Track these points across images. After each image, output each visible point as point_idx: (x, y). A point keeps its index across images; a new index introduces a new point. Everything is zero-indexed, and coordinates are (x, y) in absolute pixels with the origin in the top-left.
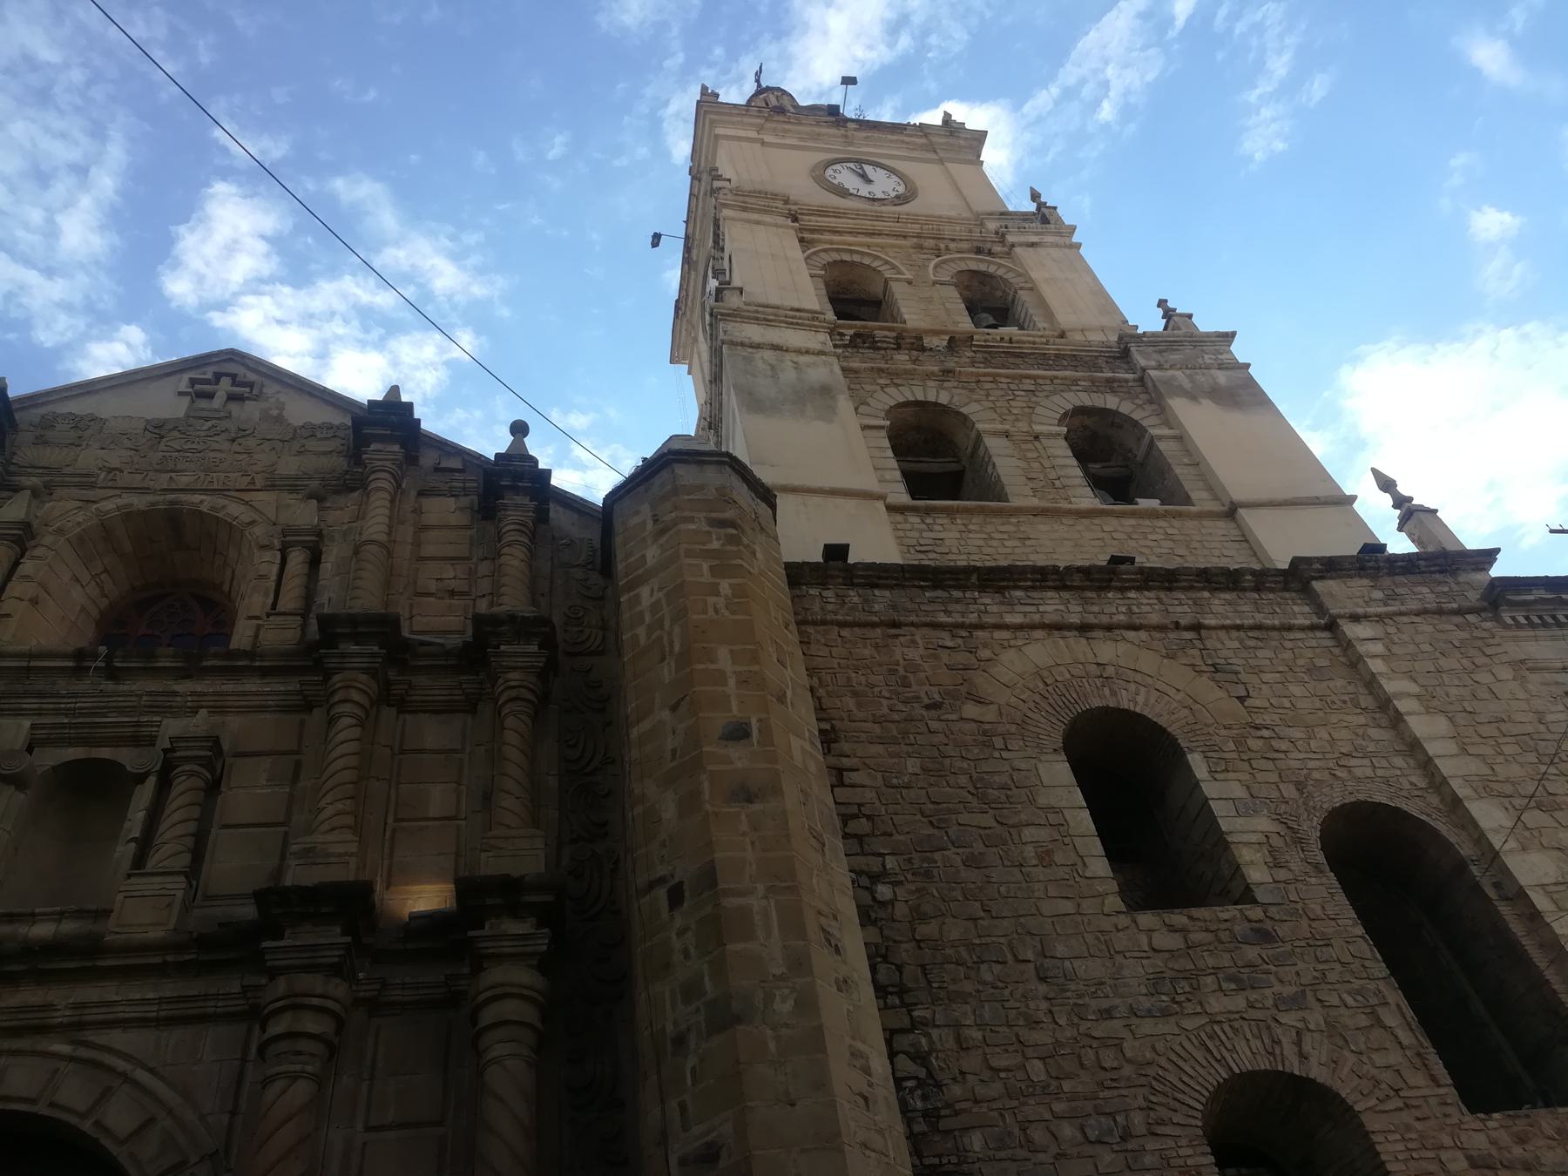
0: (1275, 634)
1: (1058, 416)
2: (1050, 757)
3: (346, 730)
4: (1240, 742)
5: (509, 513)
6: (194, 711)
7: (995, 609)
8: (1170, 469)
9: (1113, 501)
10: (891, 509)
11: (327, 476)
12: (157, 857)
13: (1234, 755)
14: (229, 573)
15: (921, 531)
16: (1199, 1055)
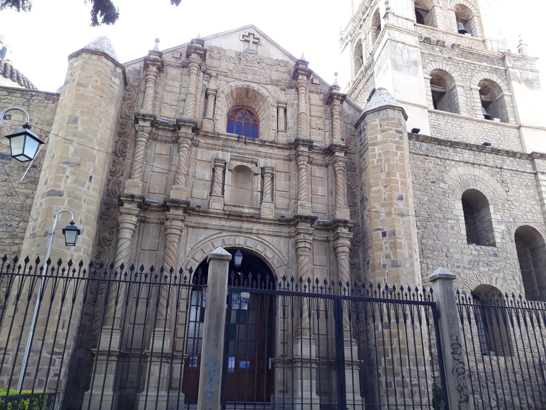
0: (520, 173)
1: (479, 82)
2: (458, 201)
3: (303, 173)
4: (503, 205)
5: (336, 107)
6: (265, 157)
7: (452, 154)
8: (506, 107)
9: (486, 113)
10: (429, 111)
11: (286, 82)
12: (266, 198)
13: (501, 208)
14: (258, 107)
15: (435, 120)
16: (475, 279)
